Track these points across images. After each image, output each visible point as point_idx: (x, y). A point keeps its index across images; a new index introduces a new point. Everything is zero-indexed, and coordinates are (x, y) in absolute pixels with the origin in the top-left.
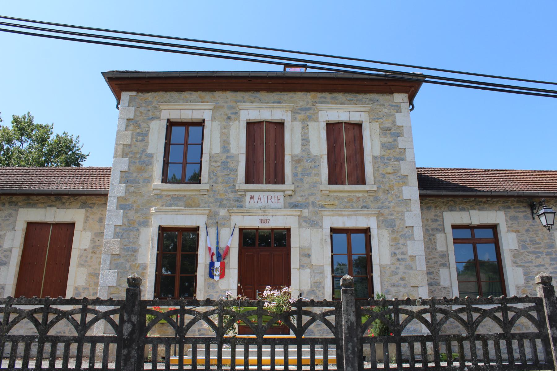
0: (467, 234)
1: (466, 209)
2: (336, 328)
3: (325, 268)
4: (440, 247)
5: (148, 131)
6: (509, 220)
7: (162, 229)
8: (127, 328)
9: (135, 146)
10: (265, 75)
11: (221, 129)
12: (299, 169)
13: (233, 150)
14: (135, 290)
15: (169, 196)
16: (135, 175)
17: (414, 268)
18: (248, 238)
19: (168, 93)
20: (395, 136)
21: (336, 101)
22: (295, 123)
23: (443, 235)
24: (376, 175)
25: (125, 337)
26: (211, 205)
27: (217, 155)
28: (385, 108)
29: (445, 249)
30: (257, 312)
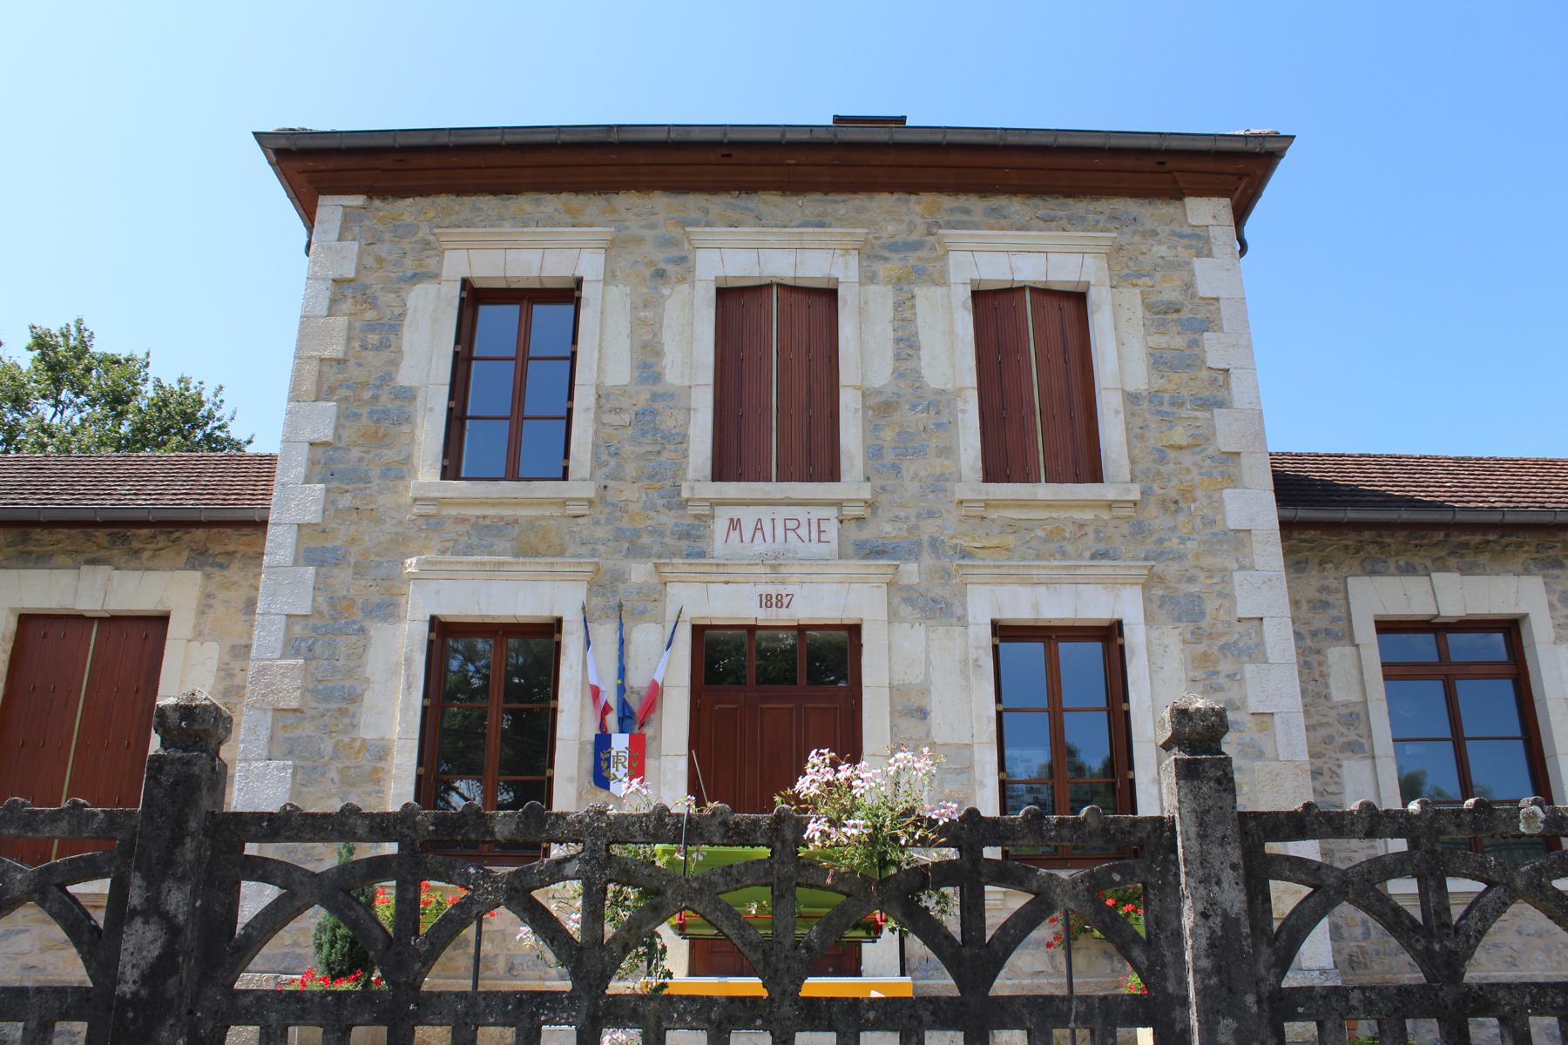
0: (1422, 647)
1: (1420, 568)
2: (1149, 943)
3: (976, 755)
4: (1342, 690)
5: (402, 315)
6: (1556, 603)
7: (443, 632)
8: (141, 943)
9: (360, 365)
11: (634, 308)
12: (888, 435)
13: (673, 376)
14: (188, 763)
15: (464, 520)
16: (355, 453)
17: (1269, 752)
18: (720, 657)
19: (466, 199)
20: (1195, 331)
21: (1003, 222)
22: (872, 288)
23: (1349, 650)
24: (1136, 451)
25: (126, 989)
26: (602, 548)
27: (623, 390)
28: (1160, 243)
29: (1355, 697)
30: (768, 872)
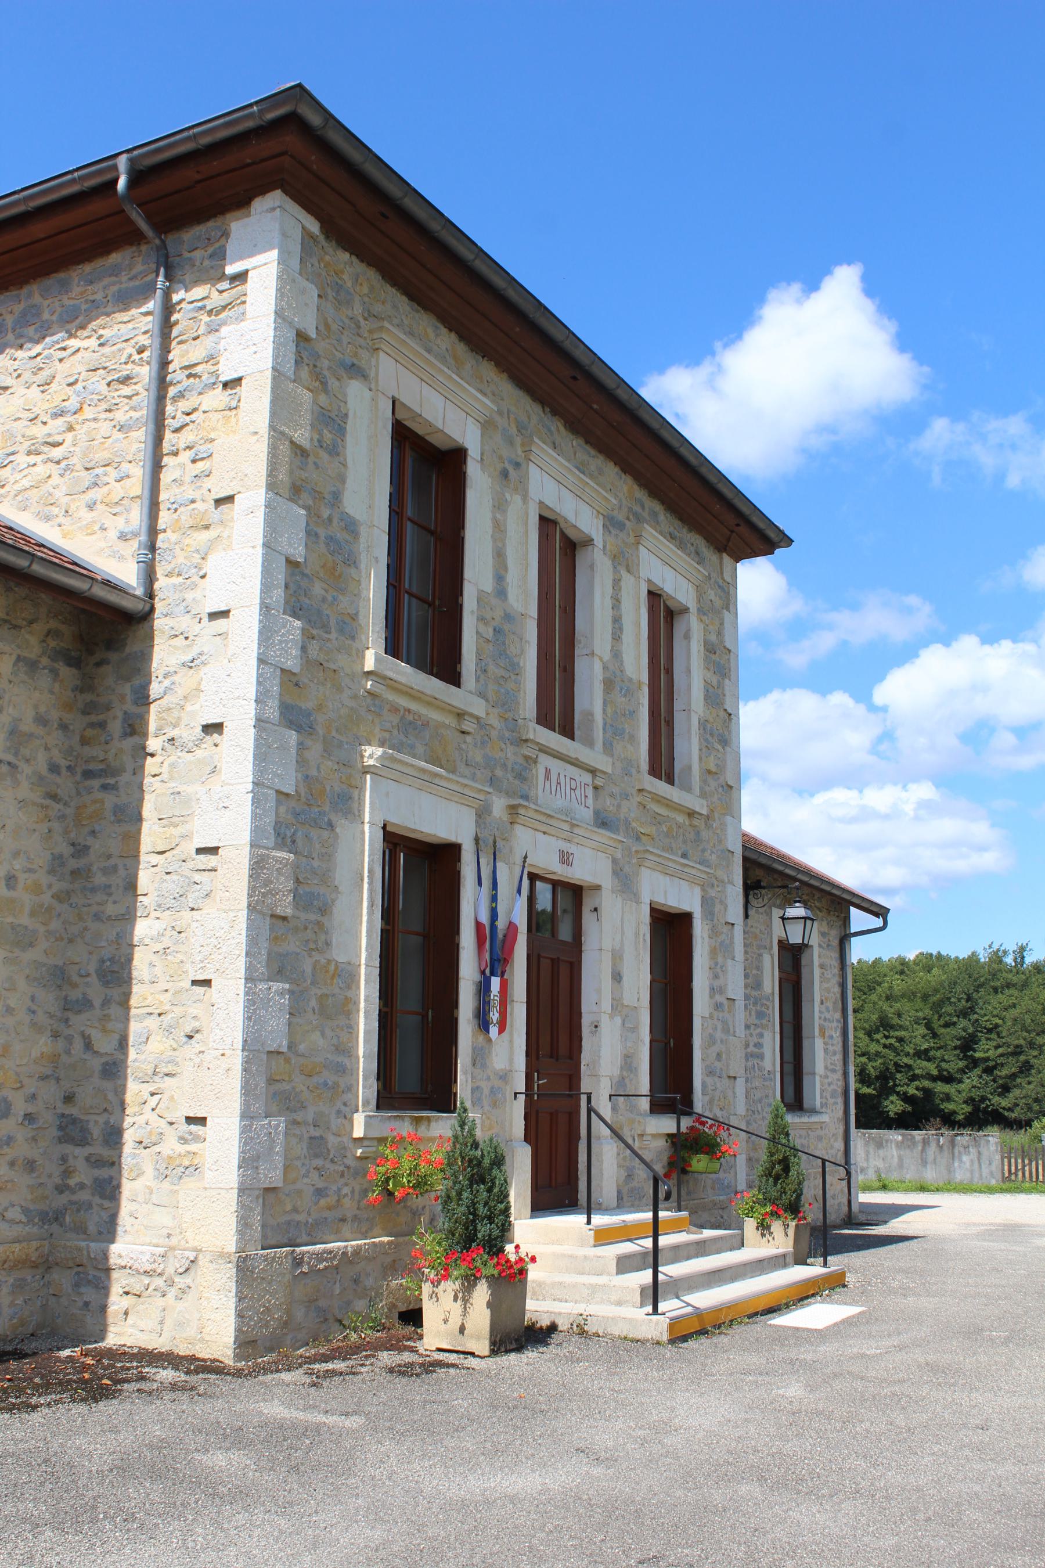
10: (610, 383)
15: (395, 709)
